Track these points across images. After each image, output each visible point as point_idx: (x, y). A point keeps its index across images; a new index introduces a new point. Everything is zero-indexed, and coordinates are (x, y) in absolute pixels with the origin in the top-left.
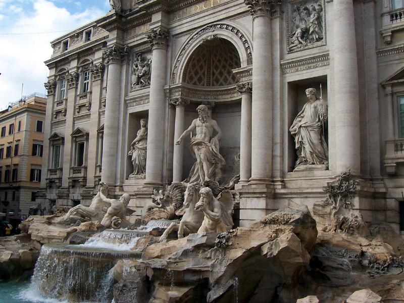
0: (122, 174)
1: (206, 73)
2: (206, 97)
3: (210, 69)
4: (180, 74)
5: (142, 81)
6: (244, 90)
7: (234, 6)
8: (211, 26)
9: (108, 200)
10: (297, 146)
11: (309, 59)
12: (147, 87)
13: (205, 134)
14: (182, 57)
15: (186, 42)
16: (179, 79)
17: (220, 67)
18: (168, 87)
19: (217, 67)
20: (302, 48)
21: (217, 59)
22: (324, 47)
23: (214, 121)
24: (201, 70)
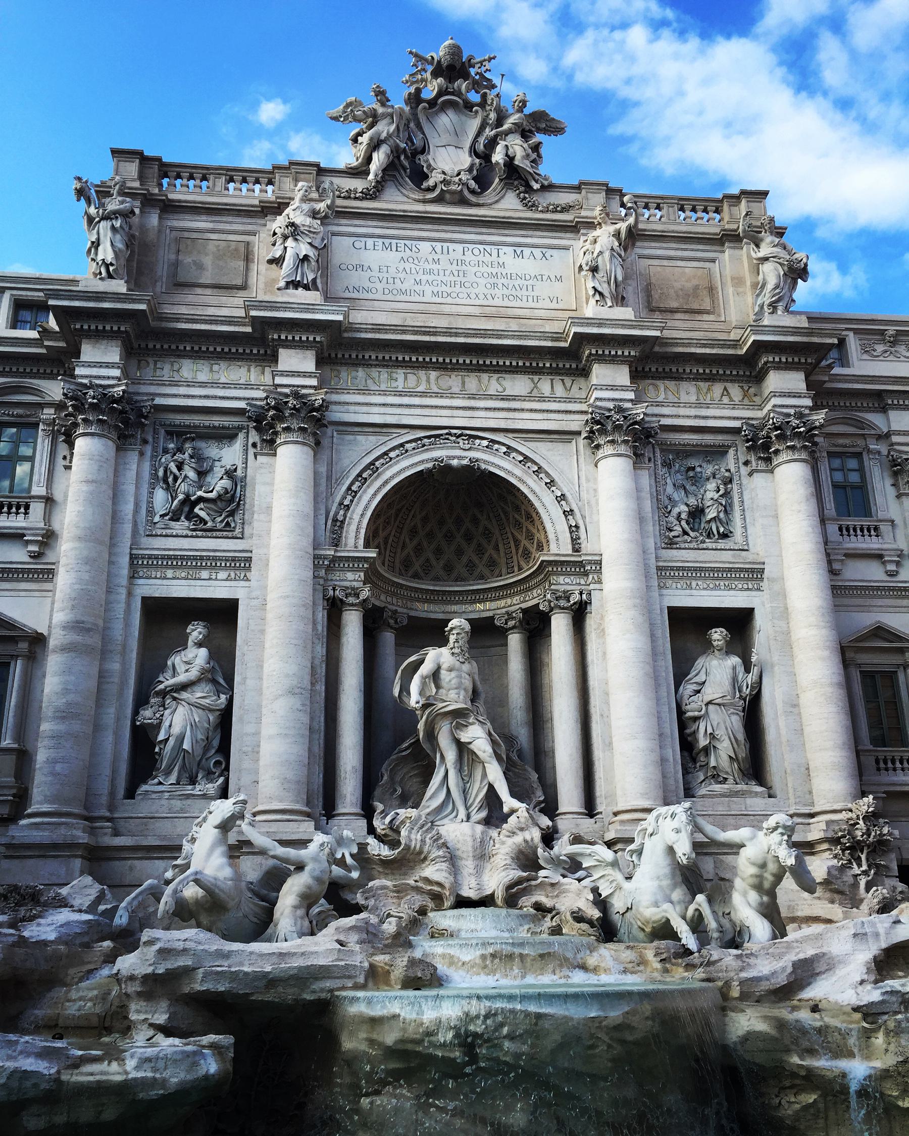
0: (113, 780)
2: (389, 599)
3: (400, 533)
5: (203, 514)
6: (567, 605)
7: (531, 410)
8: (458, 437)
9: (291, 852)
11: (718, 570)
13: (465, 690)
14: (368, 487)
16: (356, 538)
18: (333, 553)
19: (413, 532)
21: (424, 514)
23: (475, 664)
24: (383, 530)
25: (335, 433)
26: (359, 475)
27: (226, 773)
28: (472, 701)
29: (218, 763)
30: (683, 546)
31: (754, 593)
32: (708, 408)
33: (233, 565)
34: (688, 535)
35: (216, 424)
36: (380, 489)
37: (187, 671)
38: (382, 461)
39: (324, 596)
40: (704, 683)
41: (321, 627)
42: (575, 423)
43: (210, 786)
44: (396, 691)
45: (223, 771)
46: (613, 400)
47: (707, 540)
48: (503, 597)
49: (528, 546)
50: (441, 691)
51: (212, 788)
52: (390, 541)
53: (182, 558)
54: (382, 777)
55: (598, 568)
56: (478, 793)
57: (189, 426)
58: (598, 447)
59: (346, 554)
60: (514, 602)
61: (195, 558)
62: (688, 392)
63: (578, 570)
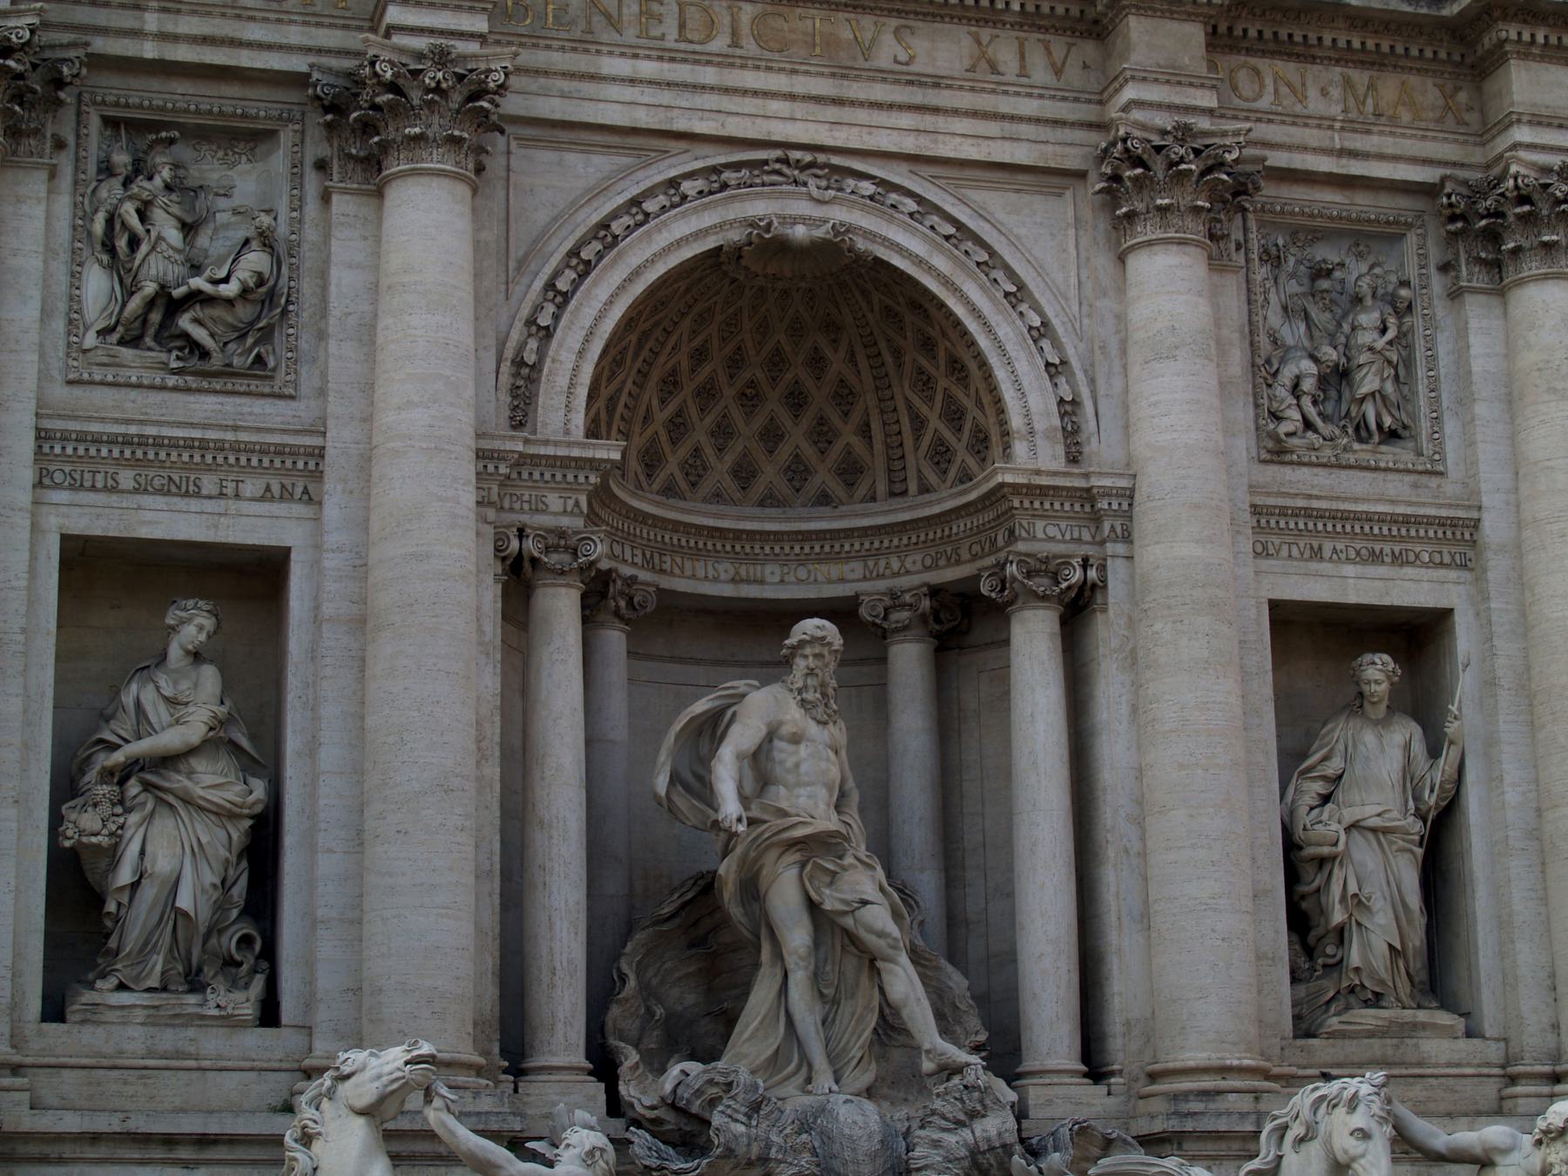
1: (624, 398)
2: (617, 549)
3: (640, 385)
4: (572, 385)
5: (200, 334)
8: (804, 167)
10: (1338, 917)
11: (1382, 519)
12: (254, 385)
14: (595, 284)
15: (620, 200)
17: (688, 389)
18: (520, 447)
19: (671, 383)
20: (1327, 453)
21: (696, 343)
22: (1434, 482)
24: (609, 380)
25: (513, 144)
26: (574, 253)
27: (265, 965)
28: (839, 808)
29: (245, 941)
30: (1306, 459)
31: (1453, 574)
32: (1368, 132)
33: (277, 463)
34: (1316, 431)
35: (228, 109)
36: (622, 288)
37: (177, 722)
38: (626, 220)
39: (497, 549)
40: (1340, 777)
41: (492, 628)
42: (1070, 151)
43: (239, 996)
44: (662, 783)
45: (257, 958)
46: (1170, 107)
47: (1356, 446)
48: (877, 554)
49: (947, 434)
50: (773, 789)
51: (245, 1003)
52: (620, 408)
53: (158, 442)
54: (623, 979)
55: (1125, 506)
56: (859, 1028)
57: (163, 109)
58: (1131, 216)
59: (550, 451)
60: (908, 566)
61: (189, 444)
62: (1323, 91)
63: (1077, 507)
